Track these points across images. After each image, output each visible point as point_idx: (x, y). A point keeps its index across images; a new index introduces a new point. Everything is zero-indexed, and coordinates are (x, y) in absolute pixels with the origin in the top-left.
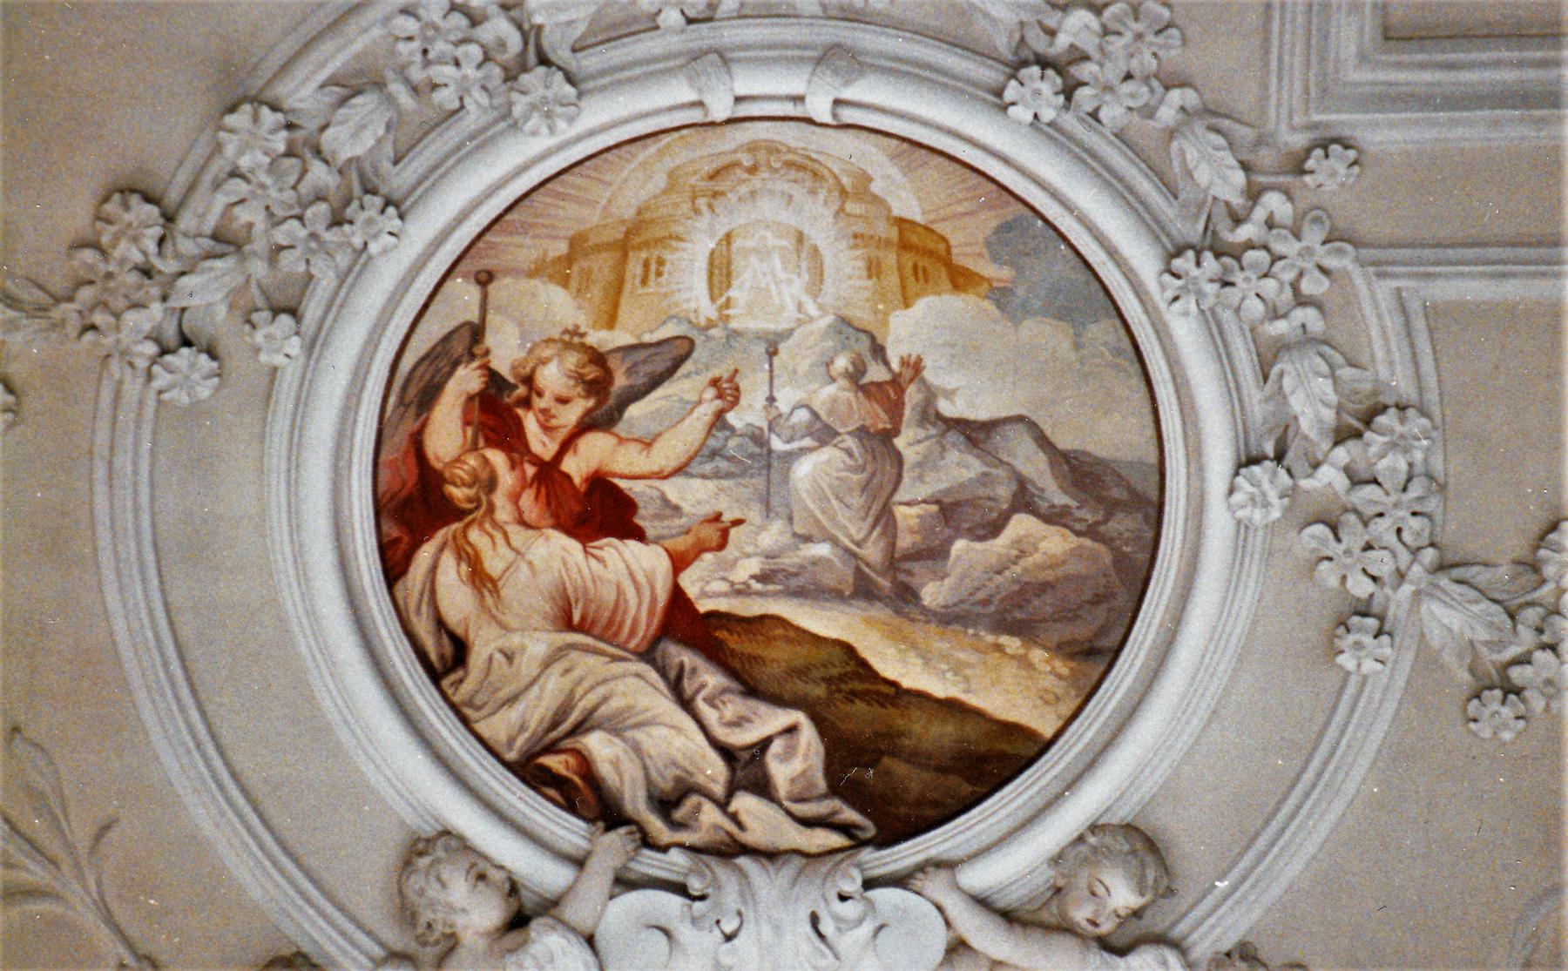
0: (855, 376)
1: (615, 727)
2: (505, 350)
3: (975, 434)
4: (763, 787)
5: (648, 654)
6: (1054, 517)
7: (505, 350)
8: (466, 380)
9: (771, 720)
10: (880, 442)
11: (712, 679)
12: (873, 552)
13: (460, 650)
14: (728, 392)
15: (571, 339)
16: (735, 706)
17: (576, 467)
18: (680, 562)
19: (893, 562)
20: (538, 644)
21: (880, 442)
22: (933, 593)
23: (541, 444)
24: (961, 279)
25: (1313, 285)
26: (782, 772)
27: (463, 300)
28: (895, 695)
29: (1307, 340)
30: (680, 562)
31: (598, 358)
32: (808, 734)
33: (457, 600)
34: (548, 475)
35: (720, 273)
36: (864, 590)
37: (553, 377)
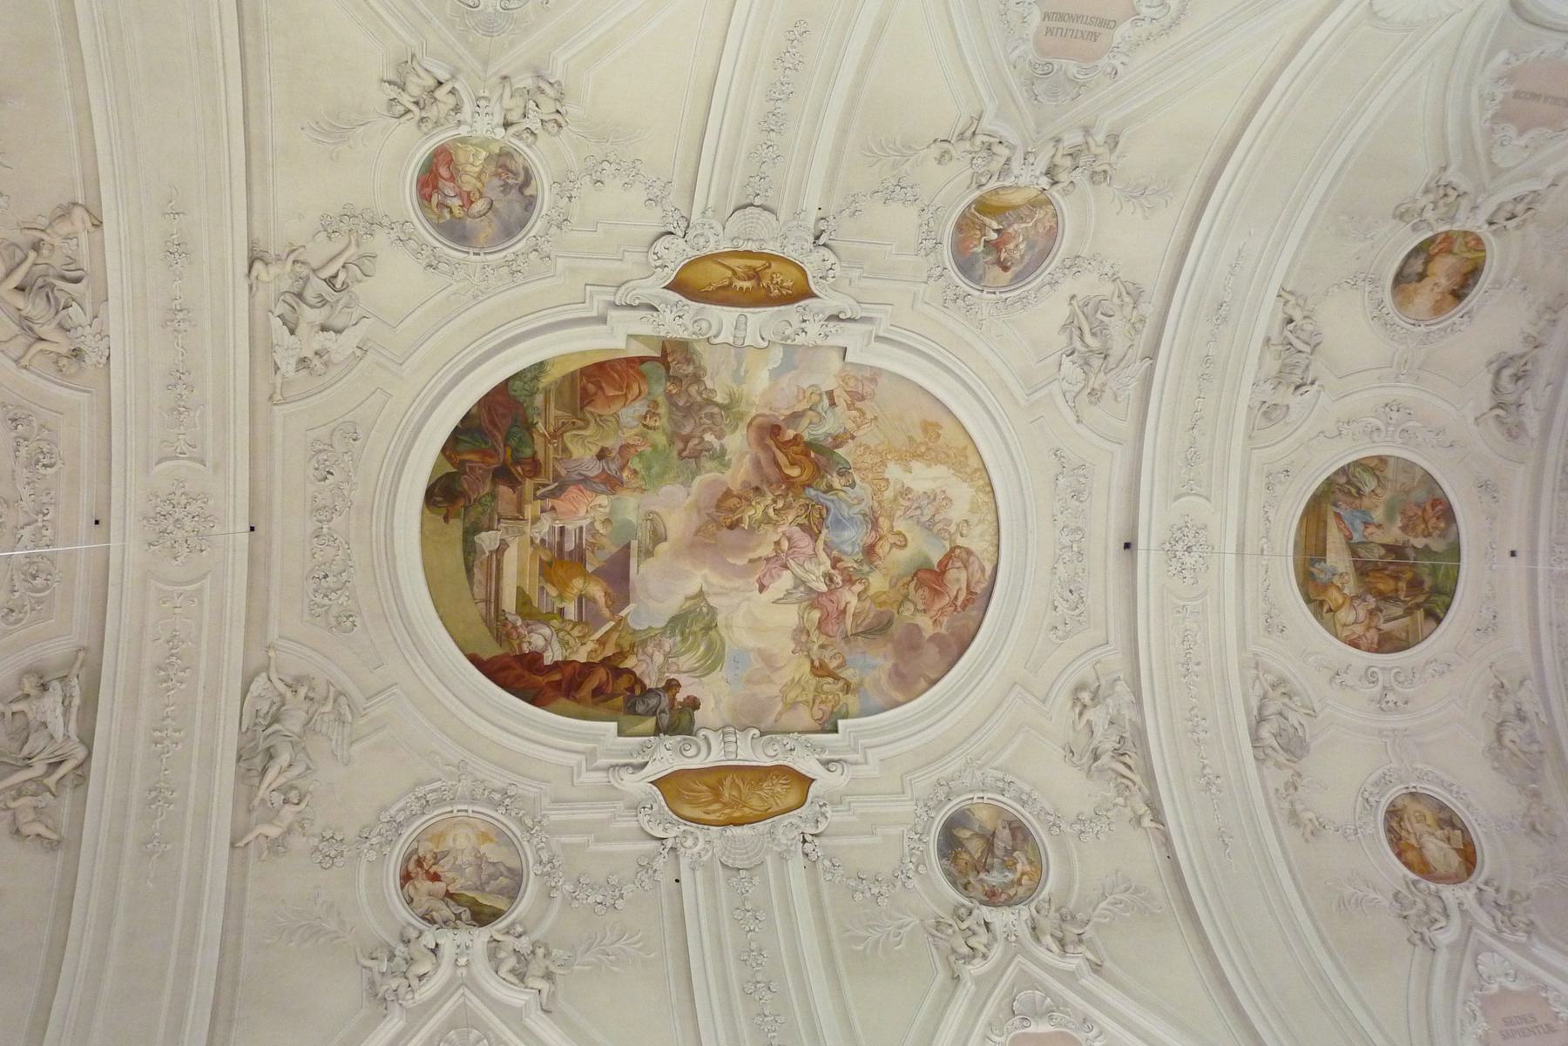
0: (475, 856)
1: (437, 911)
2: (421, 853)
3: (494, 864)
4: (461, 920)
5: (442, 900)
6: (506, 877)
7: (421, 853)
8: (415, 857)
9: (461, 909)
10: (479, 867)
11: (452, 903)
12: (478, 883)
13: (412, 900)
14: (456, 859)
15: (431, 851)
16: (456, 907)
17: (432, 871)
18: (448, 885)
19: (481, 884)
20: (424, 899)
21: (479, 867)
22: (487, 889)
23: (426, 867)
24: (491, 841)
25: (544, 840)
26: (464, 917)
27: (415, 845)
28: (481, 905)
29: (543, 848)
30: (448, 885)
31: (435, 853)
32: (468, 912)
33: (412, 892)
34: (427, 872)
35: (454, 840)
36: (477, 889)
37: (428, 856)
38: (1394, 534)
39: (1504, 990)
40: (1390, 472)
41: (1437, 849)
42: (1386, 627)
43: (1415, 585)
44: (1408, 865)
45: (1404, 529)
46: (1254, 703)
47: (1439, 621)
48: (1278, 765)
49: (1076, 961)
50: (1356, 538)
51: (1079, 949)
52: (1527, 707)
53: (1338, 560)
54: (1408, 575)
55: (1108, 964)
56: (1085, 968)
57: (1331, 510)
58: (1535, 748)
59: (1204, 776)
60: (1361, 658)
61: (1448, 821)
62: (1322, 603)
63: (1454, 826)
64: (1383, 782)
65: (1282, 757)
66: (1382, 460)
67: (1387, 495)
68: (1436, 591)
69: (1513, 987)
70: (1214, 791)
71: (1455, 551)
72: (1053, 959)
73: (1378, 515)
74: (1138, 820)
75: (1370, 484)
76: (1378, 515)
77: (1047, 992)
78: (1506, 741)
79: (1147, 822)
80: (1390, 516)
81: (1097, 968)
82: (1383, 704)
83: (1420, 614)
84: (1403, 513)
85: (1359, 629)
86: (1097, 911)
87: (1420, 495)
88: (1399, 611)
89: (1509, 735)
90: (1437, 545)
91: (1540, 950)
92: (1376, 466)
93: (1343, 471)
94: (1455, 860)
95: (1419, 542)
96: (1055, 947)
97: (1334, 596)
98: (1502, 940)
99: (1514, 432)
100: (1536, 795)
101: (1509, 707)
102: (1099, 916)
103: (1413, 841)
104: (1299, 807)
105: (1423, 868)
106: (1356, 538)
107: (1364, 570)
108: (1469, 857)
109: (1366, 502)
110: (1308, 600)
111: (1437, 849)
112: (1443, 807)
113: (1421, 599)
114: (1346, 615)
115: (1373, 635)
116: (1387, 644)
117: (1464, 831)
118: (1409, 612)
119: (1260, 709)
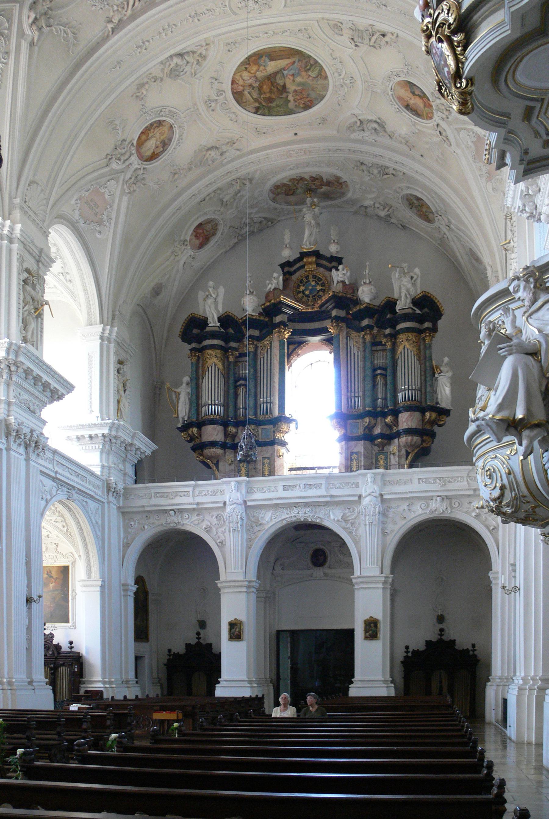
38: (291, 87)
39: (103, 194)
40: (321, 81)
41: (151, 145)
42: (246, 92)
43: (270, 100)
44: (139, 137)
45: (295, 91)
46: (189, 49)
47: (255, 113)
48: (163, 70)
49: (30, 33)
50: (285, 72)
51: (36, 32)
52: (227, 154)
53: (272, 66)
54: (274, 97)
55: (36, 48)
56: (30, 39)
57: (296, 59)
58: (210, 162)
59: (143, 43)
60: (227, 86)
61: (165, 144)
62: (249, 64)
63: (163, 147)
64: (172, 114)
65: (167, 70)
66: (326, 78)
67: (309, 81)
68: (270, 108)
69: (106, 196)
70: (138, 50)
71: (290, 112)
72: (26, 23)
73: (299, 79)
74: (110, 21)
75: (313, 74)
76: (299, 79)
77: (9, 29)
78: (209, 152)
79: (110, 26)
80: (300, 84)
81: (32, 44)
82: (209, 102)
83: (257, 105)
84: (303, 89)
85: (241, 82)
86: (58, 27)
87: (313, 95)
88: (255, 96)
89: (212, 153)
90: (291, 105)
91: (125, 199)
92: (322, 75)
93: (317, 62)
94: (149, 153)
95: (290, 98)
96: (31, 20)
97: (254, 68)
98: (123, 184)
99: (351, 128)
100: (190, 169)
101: (225, 148)
102: (55, 28)
103: (150, 135)
104: (147, 86)
105: (140, 143)
106: (285, 72)
107: (271, 78)
108: (153, 157)
109: (304, 74)
110: (249, 58)
111: (151, 145)
112: (170, 140)
113: (264, 104)
114: (246, 75)
115: (240, 88)
116: (238, 96)
117: (163, 152)
118: (256, 100)
119: (187, 53)
